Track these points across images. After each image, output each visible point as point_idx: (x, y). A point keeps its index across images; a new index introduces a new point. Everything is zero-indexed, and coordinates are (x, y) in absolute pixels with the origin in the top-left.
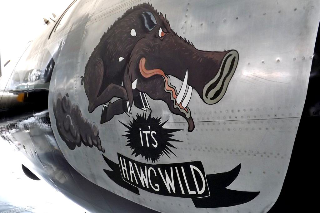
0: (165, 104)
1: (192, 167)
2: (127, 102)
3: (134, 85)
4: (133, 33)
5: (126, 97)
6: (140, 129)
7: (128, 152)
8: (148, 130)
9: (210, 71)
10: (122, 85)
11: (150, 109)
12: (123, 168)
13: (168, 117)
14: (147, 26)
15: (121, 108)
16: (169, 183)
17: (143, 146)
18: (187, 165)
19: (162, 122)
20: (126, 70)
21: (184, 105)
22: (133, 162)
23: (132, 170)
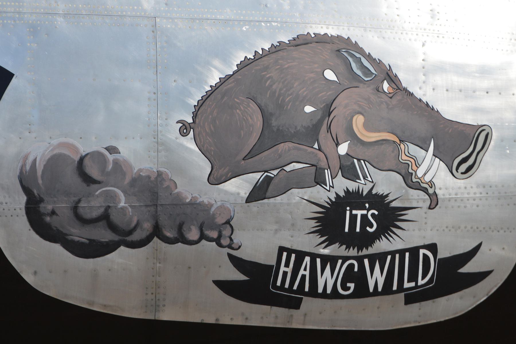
2: (326, 171)
5: (323, 164)
6: (348, 208)
10: (316, 146)
11: (373, 182)
12: (283, 269)
17: (347, 230)
20: (324, 127)
23: (305, 270)
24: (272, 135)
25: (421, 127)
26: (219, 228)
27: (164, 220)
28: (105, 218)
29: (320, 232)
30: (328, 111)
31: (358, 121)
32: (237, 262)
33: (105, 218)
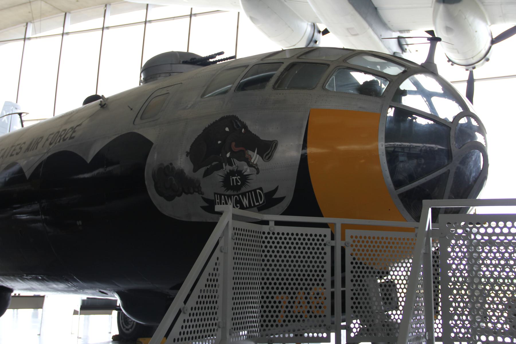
0: (246, 163)
1: (258, 191)
3: (228, 155)
4: (227, 129)
7: (222, 190)
8: (235, 176)
9: (267, 148)
12: (217, 201)
13: (247, 169)
14: (235, 127)
15: (219, 167)
16: (245, 202)
18: (255, 191)
19: (243, 171)
21: (255, 163)
22: (224, 195)
29: (224, 186)
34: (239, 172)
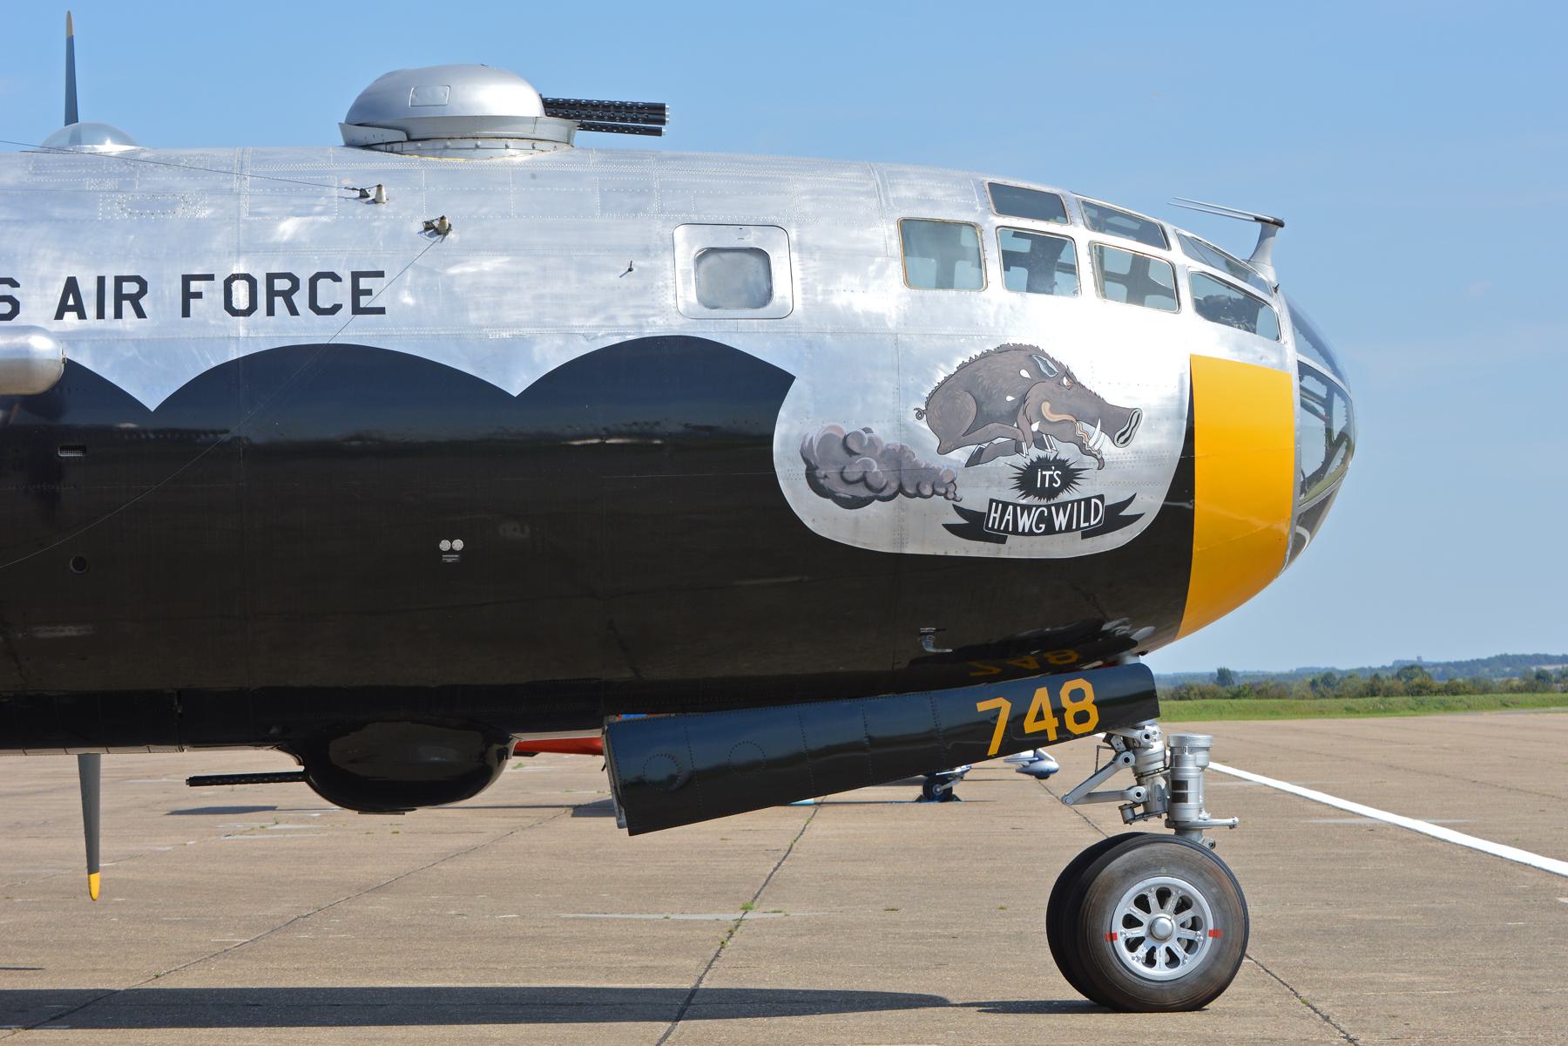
5: (1021, 438)
7: (1013, 495)
16: (1060, 520)
18: (1088, 501)
22: (1015, 506)
24: (983, 418)
25: (1092, 410)
26: (946, 486)
27: (906, 482)
28: (863, 480)
30: (1023, 399)
31: (1046, 407)
32: (960, 511)
33: (863, 480)
34: (1061, 464)
